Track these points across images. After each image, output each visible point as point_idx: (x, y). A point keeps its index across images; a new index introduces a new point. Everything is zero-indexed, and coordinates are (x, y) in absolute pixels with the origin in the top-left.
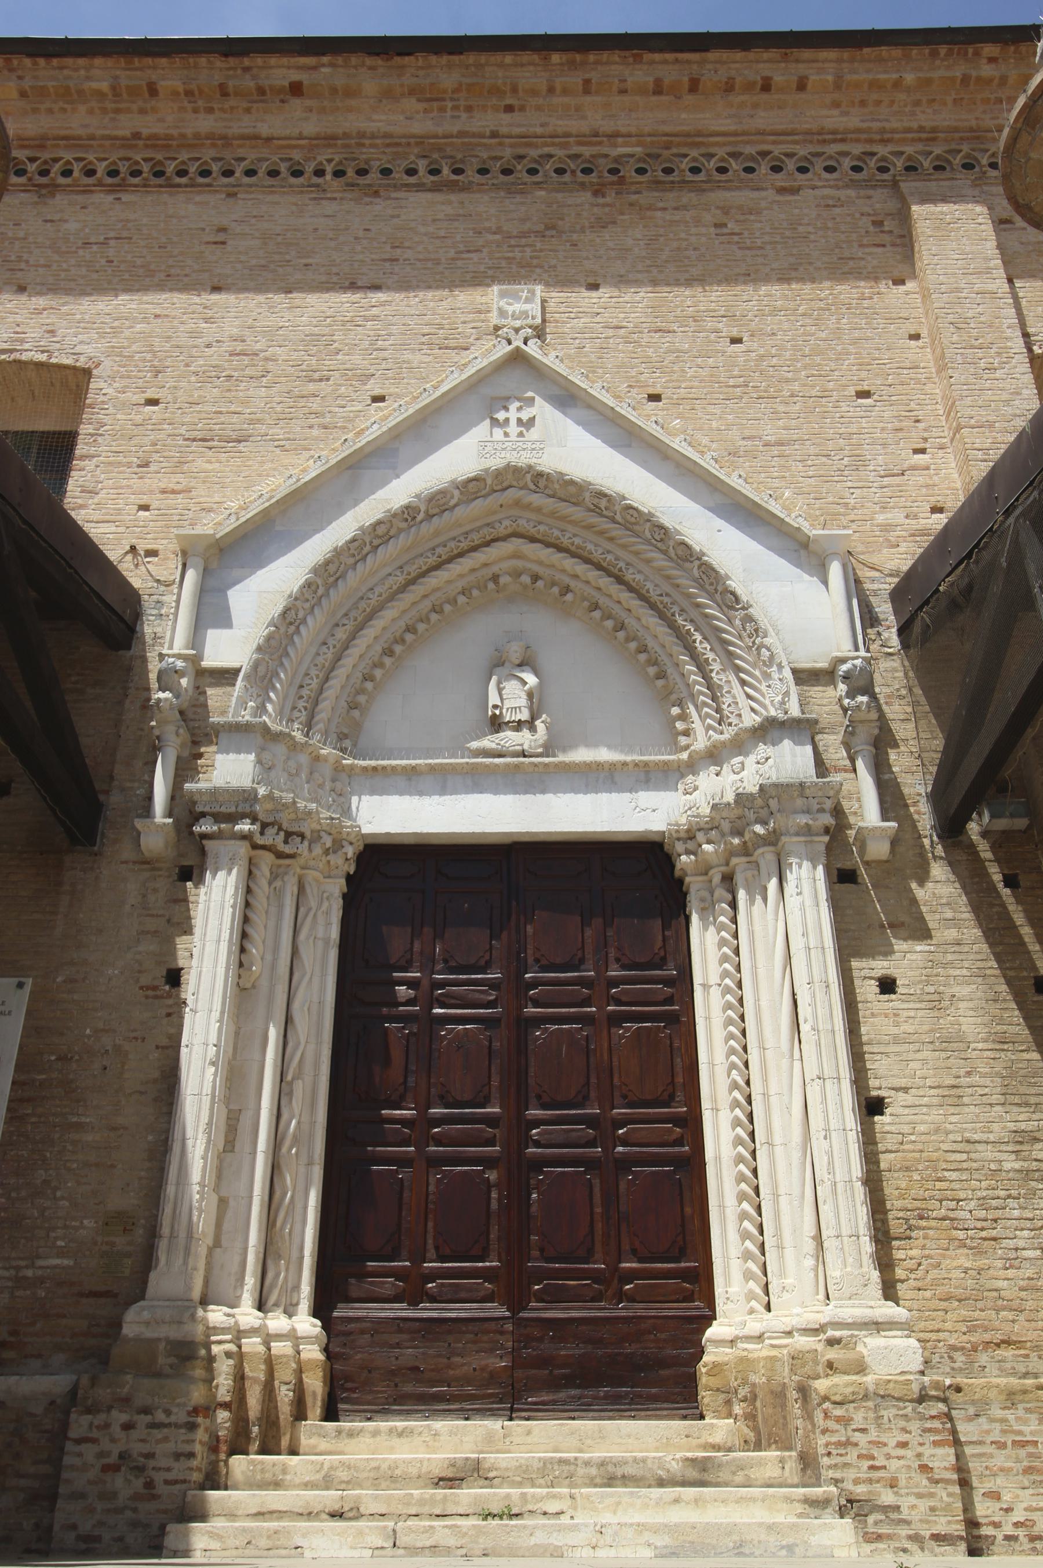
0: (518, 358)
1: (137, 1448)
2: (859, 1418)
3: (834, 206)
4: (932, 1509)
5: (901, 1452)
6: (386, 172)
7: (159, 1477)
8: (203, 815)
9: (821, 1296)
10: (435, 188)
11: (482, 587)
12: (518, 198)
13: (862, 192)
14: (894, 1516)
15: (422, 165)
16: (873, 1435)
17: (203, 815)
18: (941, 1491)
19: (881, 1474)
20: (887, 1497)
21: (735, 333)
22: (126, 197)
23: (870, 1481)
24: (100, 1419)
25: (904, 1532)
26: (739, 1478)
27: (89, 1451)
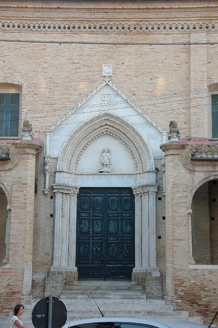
0: (107, 84)
1: (55, 285)
2: (150, 282)
3: (176, 40)
4: (158, 294)
5: (155, 286)
6: (79, 28)
7: (58, 289)
8: (55, 189)
9: (148, 265)
10: (90, 33)
11: (100, 134)
12: (108, 36)
13: (183, 35)
14: (153, 294)
15: (87, 26)
16: (152, 284)
17: (55, 189)
18: (160, 291)
19: (152, 289)
20: (152, 292)
21: (151, 77)
22: (23, 34)
23: (151, 290)
24: (49, 282)
25: (154, 296)
26: (135, 289)
27: (48, 286)
